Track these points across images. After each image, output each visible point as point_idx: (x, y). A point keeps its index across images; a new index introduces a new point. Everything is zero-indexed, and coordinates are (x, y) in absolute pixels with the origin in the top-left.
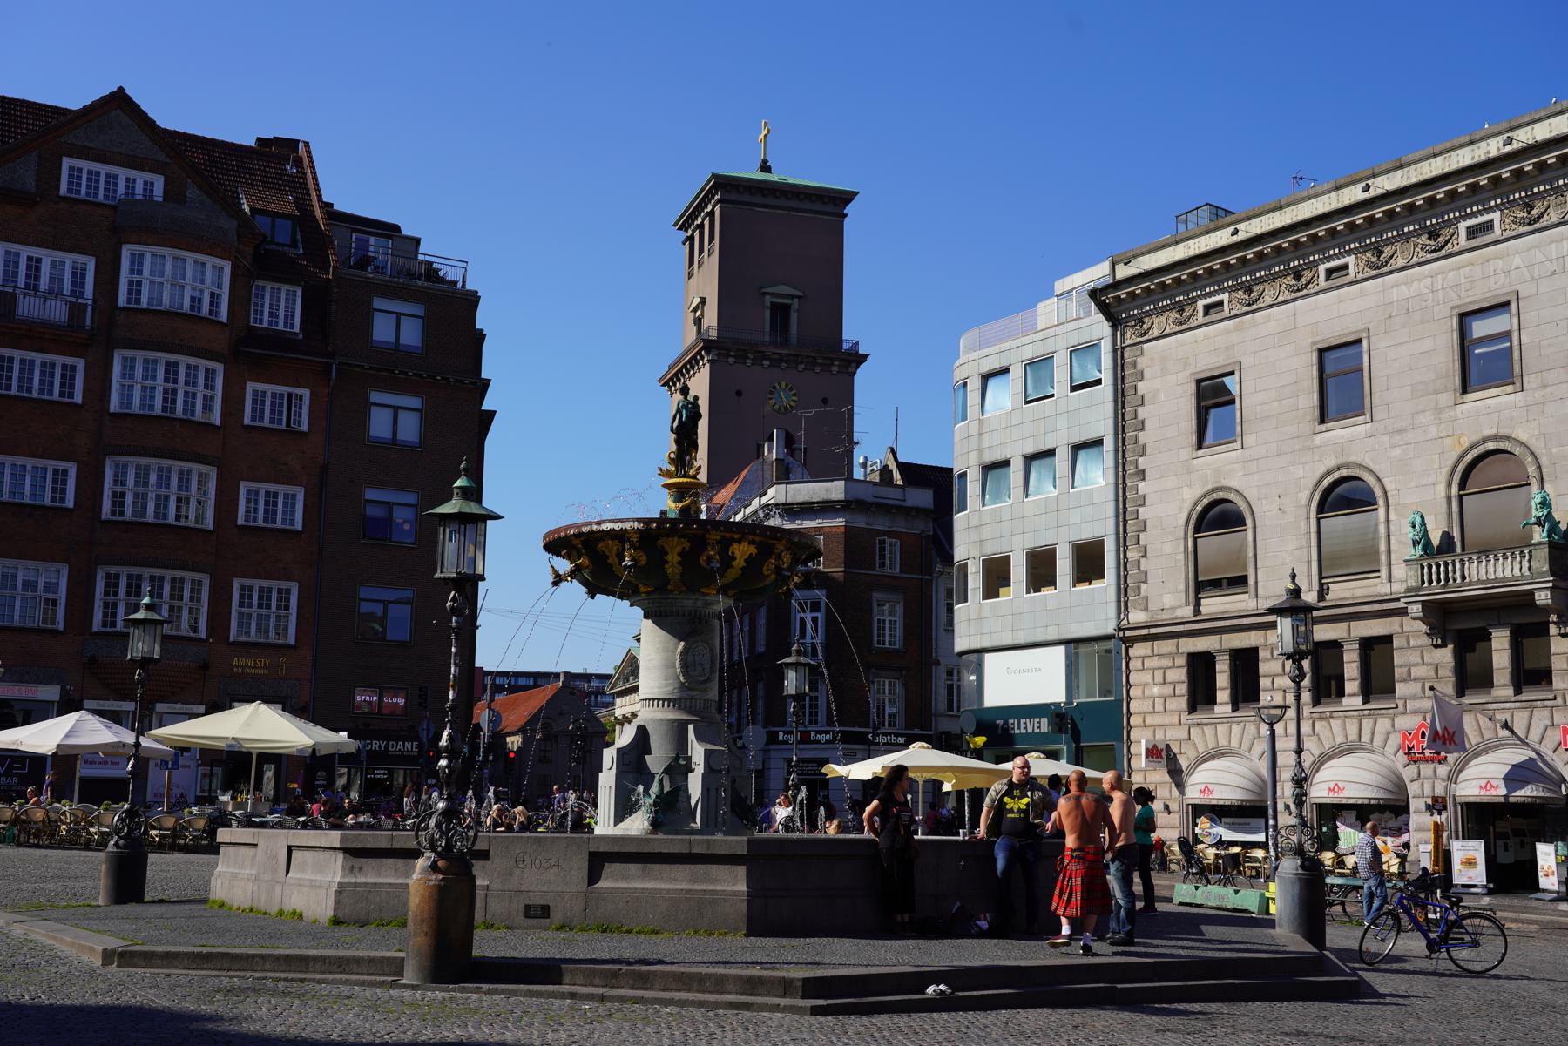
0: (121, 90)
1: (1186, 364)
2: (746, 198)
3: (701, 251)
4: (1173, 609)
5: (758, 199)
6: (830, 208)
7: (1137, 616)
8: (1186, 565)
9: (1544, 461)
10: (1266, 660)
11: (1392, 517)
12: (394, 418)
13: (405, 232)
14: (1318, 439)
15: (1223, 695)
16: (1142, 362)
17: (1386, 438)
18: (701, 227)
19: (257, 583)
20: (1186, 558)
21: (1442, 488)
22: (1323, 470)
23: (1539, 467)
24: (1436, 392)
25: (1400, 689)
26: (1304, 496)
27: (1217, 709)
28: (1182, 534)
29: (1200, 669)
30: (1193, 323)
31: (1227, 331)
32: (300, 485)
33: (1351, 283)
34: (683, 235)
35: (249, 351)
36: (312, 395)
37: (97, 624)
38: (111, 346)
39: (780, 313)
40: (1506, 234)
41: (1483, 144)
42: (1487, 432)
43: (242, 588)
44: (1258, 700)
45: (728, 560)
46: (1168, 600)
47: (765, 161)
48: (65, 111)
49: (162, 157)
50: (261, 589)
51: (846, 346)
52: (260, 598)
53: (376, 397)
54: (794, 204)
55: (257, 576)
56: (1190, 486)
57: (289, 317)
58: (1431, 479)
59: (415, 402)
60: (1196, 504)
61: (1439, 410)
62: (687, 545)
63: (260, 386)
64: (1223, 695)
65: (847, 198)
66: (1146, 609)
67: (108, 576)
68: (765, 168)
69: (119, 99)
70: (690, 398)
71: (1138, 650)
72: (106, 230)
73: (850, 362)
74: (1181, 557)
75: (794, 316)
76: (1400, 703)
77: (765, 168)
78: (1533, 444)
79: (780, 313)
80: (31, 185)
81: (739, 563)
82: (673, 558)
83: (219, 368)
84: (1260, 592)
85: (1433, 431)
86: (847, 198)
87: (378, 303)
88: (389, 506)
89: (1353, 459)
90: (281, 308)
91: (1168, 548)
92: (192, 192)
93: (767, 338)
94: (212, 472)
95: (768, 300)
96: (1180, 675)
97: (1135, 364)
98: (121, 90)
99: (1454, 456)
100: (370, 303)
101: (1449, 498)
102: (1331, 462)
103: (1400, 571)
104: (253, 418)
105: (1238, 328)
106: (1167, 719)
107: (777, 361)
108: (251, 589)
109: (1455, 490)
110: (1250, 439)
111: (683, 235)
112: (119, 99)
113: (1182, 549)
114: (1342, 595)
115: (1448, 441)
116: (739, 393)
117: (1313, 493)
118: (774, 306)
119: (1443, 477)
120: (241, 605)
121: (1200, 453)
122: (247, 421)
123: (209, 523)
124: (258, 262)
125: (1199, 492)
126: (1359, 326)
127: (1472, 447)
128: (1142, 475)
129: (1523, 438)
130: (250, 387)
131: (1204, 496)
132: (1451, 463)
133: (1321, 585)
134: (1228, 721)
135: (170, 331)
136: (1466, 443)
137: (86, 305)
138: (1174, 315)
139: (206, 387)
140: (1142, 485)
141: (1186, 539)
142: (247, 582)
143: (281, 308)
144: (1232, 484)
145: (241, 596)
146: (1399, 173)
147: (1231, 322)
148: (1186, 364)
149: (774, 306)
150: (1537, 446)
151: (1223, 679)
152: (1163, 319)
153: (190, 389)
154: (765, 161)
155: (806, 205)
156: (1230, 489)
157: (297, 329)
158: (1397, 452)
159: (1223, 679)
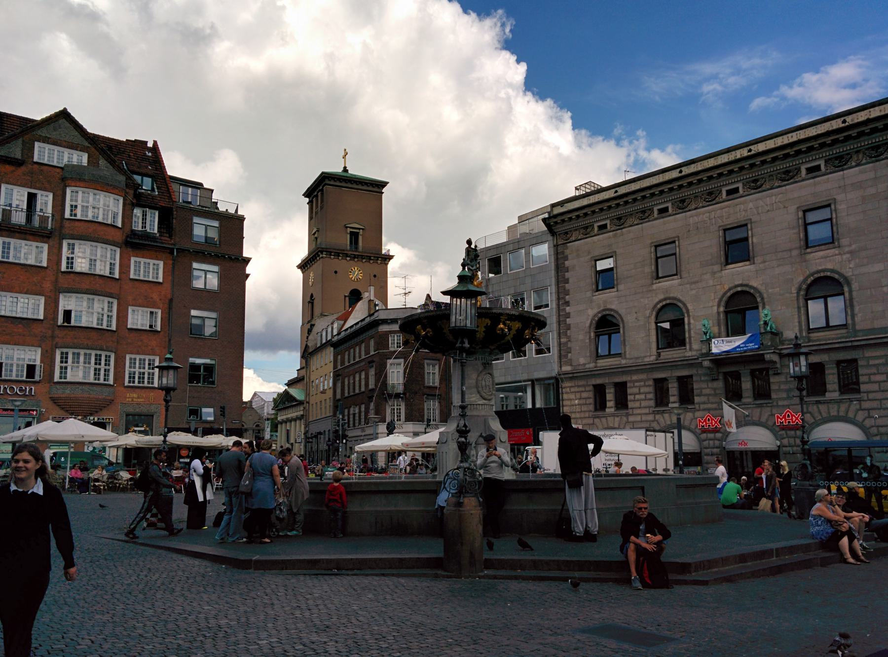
0: (65, 109)
1: (589, 253)
2: (338, 183)
3: (317, 207)
4: (584, 364)
5: (343, 184)
6: (376, 189)
7: (566, 368)
9: (765, 296)
10: (631, 387)
11: (692, 321)
12: (206, 277)
13: (205, 186)
14: (654, 287)
16: (567, 252)
17: (688, 286)
18: (317, 196)
19: (138, 357)
21: (715, 308)
22: (657, 300)
23: (763, 299)
24: (712, 265)
25: (697, 399)
27: (607, 410)
29: (599, 390)
31: (610, 238)
32: (158, 308)
33: (670, 215)
34: (307, 200)
35: (134, 243)
37: (57, 378)
38: (62, 237)
39: (354, 236)
40: (746, 193)
41: (733, 153)
42: (737, 283)
43: (131, 359)
46: (582, 361)
47: (345, 168)
48: (33, 121)
49: (87, 144)
50: (140, 360)
51: (384, 252)
52: (140, 364)
53: (195, 265)
54: (360, 187)
55: (138, 353)
57: (152, 225)
58: (711, 304)
59: (216, 268)
61: (714, 273)
63: (138, 259)
65: (383, 184)
66: (571, 365)
67: (62, 353)
68: (345, 170)
69: (64, 115)
70: (473, 246)
71: (567, 384)
72: (63, 179)
73: (386, 259)
75: (360, 238)
76: (697, 406)
77: (345, 170)
78: (759, 287)
79: (354, 236)
80: (18, 155)
83: (118, 250)
85: (711, 283)
86: (383, 184)
87: (196, 220)
88: (203, 318)
89: (672, 295)
90: (149, 222)
91: (581, 337)
92: (102, 162)
93: (348, 248)
94: (115, 302)
95: (349, 230)
96: (589, 394)
97: (563, 253)
98: (65, 109)
99: (721, 293)
100: (192, 220)
101: (718, 313)
102: (661, 297)
103: (696, 346)
105: (615, 236)
106: (582, 415)
107: (354, 257)
108: (135, 359)
109: (722, 309)
110: (621, 287)
111: (307, 200)
112: (64, 115)
115: (718, 287)
116: (336, 272)
118: (352, 233)
119: (716, 304)
120: (130, 367)
122: (132, 276)
123: (114, 328)
124: (136, 200)
125: (596, 311)
126: (674, 235)
127: (730, 289)
128: (567, 303)
129: (755, 285)
130: (133, 259)
131: (599, 313)
132: (719, 297)
134: (613, 415)
135: (93, 232)
136: (727, 287)
137: (48, 217)
138: (582, 231)
140: (568, 309)
142: (133, 356)
143: (149, 222)
144: (613, 307)
145: (130, 363)
146: (693, 166)
147: (611, 234)
149: (352, 233)
150: (762, 288)
151: (610, 396)
154: (345, 168)
155: (365, 187)
156: (611, 310)
157: (156, 231)
158: (694, 292)
159: (610, 396)
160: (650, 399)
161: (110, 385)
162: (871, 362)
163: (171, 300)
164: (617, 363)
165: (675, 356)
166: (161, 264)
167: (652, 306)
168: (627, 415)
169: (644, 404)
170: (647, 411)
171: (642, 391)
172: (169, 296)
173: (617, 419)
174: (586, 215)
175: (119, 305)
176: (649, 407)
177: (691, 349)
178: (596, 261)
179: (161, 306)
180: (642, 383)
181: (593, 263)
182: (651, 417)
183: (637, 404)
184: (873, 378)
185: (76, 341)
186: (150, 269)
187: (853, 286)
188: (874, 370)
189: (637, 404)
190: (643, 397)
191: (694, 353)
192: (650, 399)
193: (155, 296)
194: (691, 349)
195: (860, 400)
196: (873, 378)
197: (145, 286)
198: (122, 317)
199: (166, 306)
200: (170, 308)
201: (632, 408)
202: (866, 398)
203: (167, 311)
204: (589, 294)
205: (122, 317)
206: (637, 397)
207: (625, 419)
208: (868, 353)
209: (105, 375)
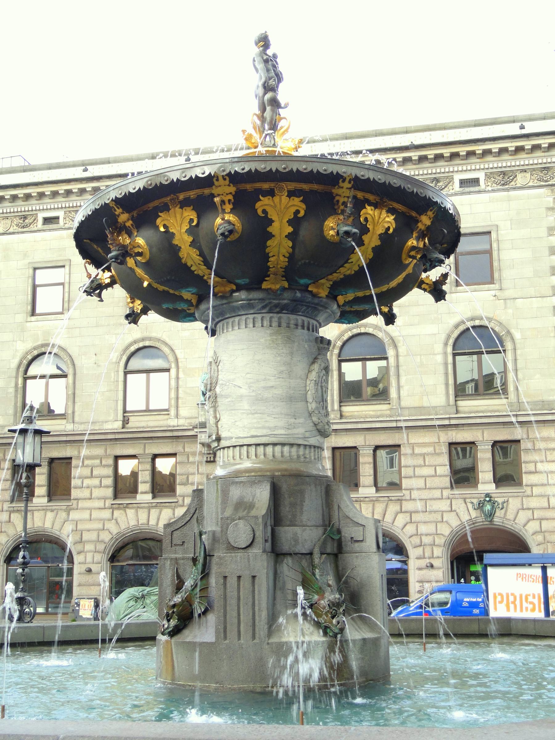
8: (16, 397)
11: (181, 375)
15: (41, 490)
20: (16, 391)
26: (114, 356)
27: (35, 500)
28: (14, 374)
30: (33, 228)
44: (70, 494)
56: (23, 341)
60: (27, 353)
64: (41, 490)
74: (12, 390)
84: (77, 419)
89: (154, 335)
113: (13, 384)
114: (138, 425)
117: (122, 355)
121: (33, 318)
131: (35, 348)
133: (124, 416)
134: (45, 509)
138: (17, 221)
141: (17, 377)
148: (25, 255)
151: (41, 478)
152: (9, 221)
159: (41, 478)
160: (107, 487)
162: (417, 450)
164: (62, 427)
165: (151, 424)
167: (121, 347)
168: (68, 510)
169: (97, 493)
170: (101, 504)
171: (95, 472)
173: (50, 515)
174: (28, 197)
176: (105, 499)
177: (177, 416)
178: (35, 269)
180: (97, 462)
181: (31, 271)
182: (106, 514)
183: (86, 493)
184: (418, 471)
187: (400, 350)
188: (420, 461)
189: (86, 493)
190: (96, 482)
191: (181, 422)
192: (107, 487)
194: (177, 416)
195: (400, 500)
196: (418, 471)
201: (77, 499)
202: (408, 498)
204: (20, 318)
206: (87, 482)
207: (63, 515)
208: (416, 438)
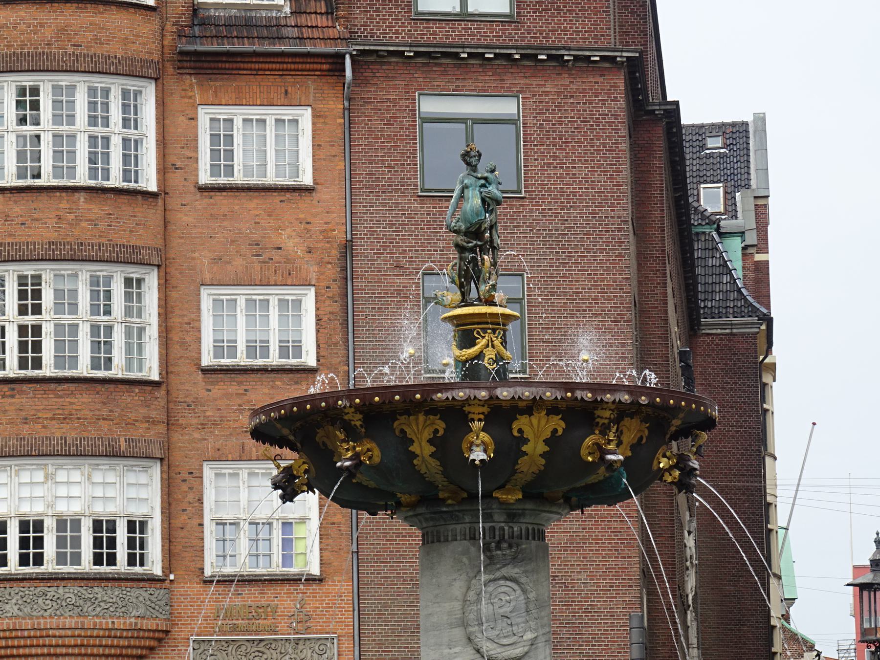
36: (316, 116)
45: (508, 449)
53: (429, 106)
59: (507, 107)
62: (441, 426)
63: (223, 112)
81: (535, 448)
82: (423, 448)
94: (152, 281)
104: (215, 170)
130: (204, 115)
139: (126, 123)
153: (99, 131)
161: (152, 580)
163: (348, 248)
166: (305, 116)
172: (340, 235)
175: (165, 286)
179: (313, 271)
185: (25, 430)
186: (273, 140)
193: (292, 243)
197: (254, 204)
198: (177, 328)
199: (332, 271)
200: (345, 275)
203: (335, 289)
205: (177, 328)
209: (131, 543)
